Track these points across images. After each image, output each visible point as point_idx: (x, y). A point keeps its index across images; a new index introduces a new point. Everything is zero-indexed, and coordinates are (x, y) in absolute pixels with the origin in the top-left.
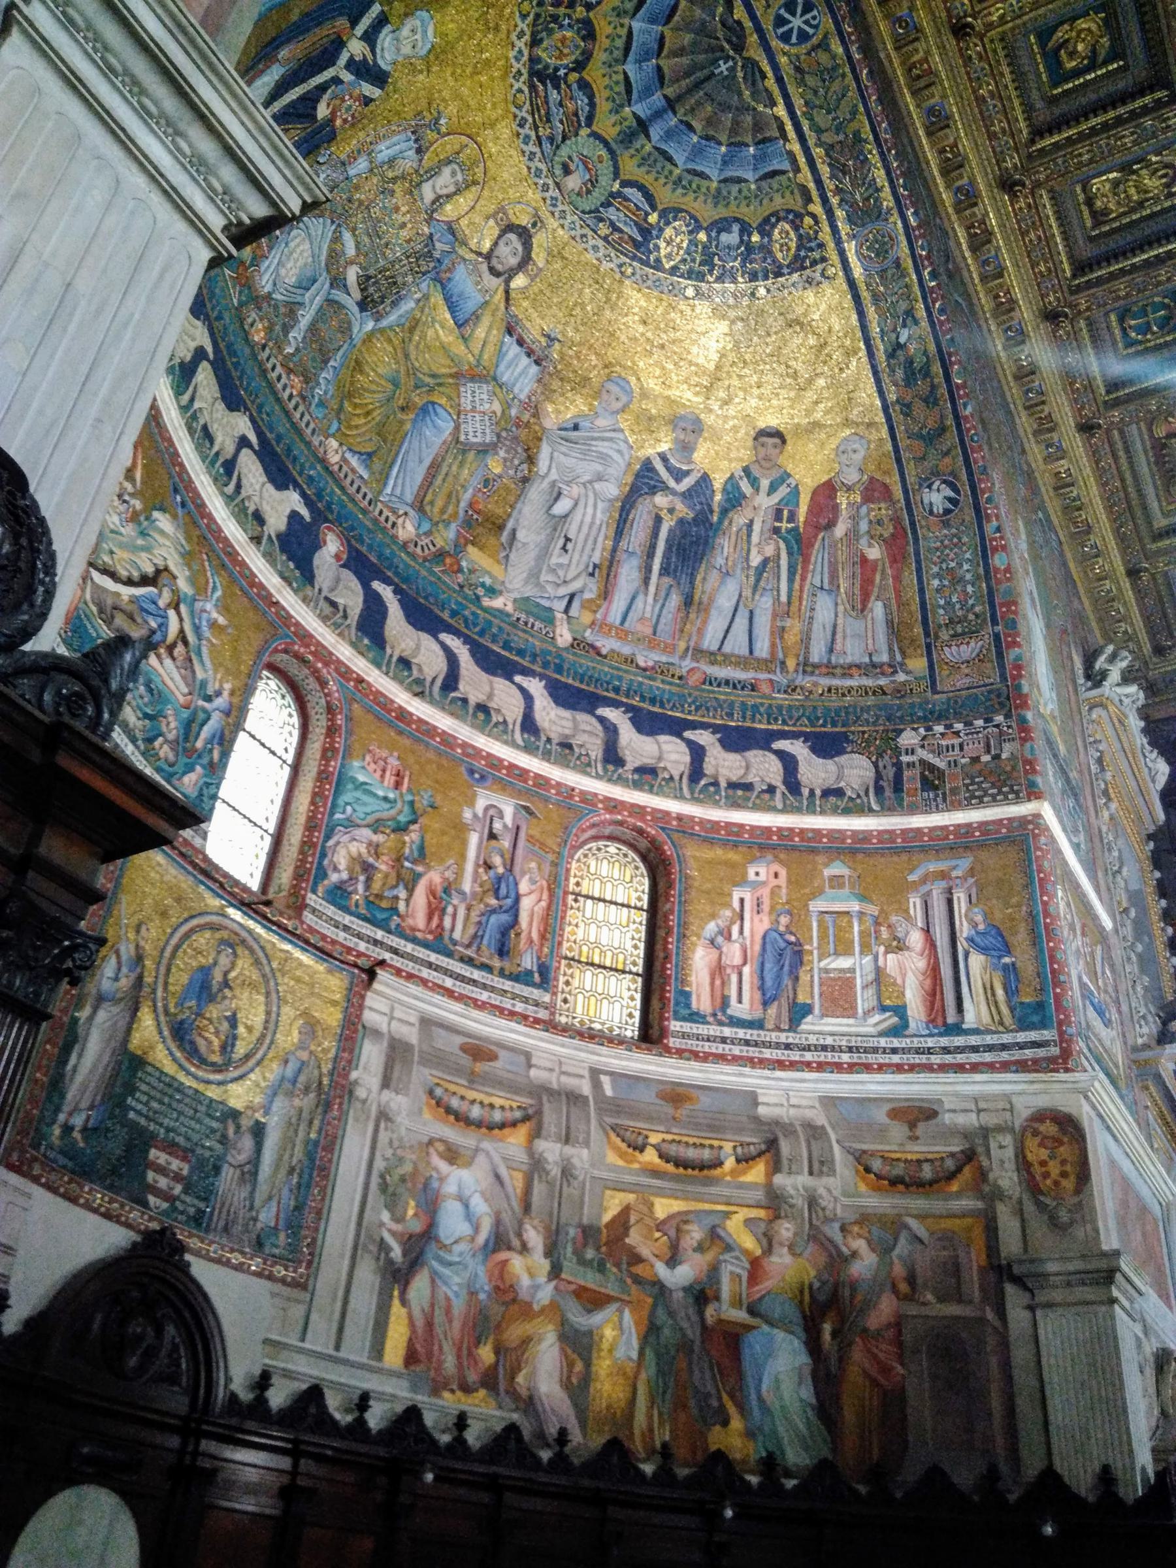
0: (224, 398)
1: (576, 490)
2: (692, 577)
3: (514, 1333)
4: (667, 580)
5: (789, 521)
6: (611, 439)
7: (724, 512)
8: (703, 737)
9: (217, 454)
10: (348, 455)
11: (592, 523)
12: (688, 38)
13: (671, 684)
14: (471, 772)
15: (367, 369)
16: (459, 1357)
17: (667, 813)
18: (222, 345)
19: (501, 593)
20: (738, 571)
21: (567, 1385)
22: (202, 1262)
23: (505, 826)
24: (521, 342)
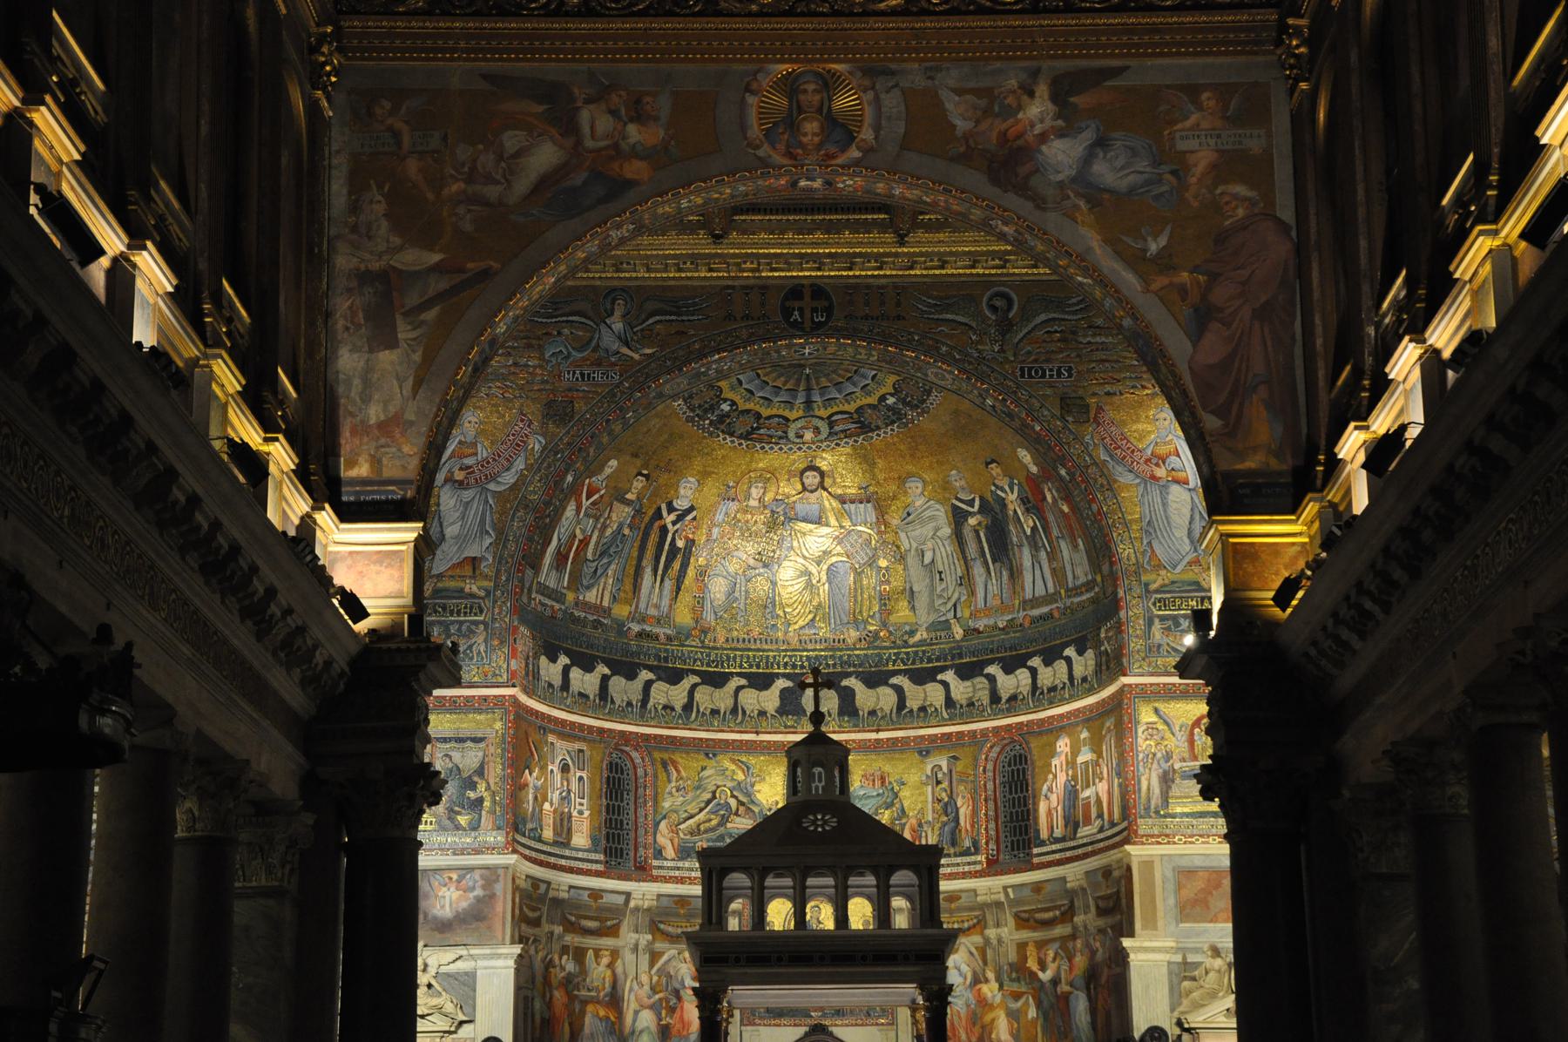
0: (716, 687)
1: (930, 544)
2: (1008, 556)
3: (988, 1018)
4: (996, 564)
5: (1029, 502)
6: (929, 508)
7: (1001, 511)
8: (1036, 662)
9: (725, 713)
10: (801, 632)
11: (948, 556)
12: (782, 379)
13: (1016, 632)
14: (920, 753)
15: (787, 584)
16: (967, 1033)
17: (1022, 723)
18: (704, 668)
19: (917, 630)
20: (1025, 541)
21: (1012, 1034)
22: (839, 1028)
23: (944, 773)
24: (852, 502)
